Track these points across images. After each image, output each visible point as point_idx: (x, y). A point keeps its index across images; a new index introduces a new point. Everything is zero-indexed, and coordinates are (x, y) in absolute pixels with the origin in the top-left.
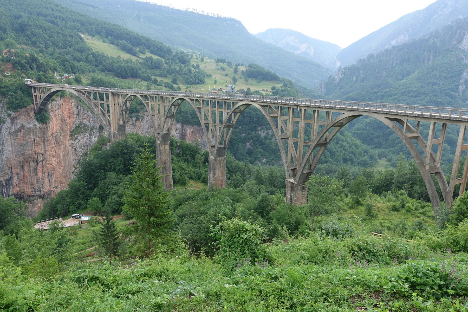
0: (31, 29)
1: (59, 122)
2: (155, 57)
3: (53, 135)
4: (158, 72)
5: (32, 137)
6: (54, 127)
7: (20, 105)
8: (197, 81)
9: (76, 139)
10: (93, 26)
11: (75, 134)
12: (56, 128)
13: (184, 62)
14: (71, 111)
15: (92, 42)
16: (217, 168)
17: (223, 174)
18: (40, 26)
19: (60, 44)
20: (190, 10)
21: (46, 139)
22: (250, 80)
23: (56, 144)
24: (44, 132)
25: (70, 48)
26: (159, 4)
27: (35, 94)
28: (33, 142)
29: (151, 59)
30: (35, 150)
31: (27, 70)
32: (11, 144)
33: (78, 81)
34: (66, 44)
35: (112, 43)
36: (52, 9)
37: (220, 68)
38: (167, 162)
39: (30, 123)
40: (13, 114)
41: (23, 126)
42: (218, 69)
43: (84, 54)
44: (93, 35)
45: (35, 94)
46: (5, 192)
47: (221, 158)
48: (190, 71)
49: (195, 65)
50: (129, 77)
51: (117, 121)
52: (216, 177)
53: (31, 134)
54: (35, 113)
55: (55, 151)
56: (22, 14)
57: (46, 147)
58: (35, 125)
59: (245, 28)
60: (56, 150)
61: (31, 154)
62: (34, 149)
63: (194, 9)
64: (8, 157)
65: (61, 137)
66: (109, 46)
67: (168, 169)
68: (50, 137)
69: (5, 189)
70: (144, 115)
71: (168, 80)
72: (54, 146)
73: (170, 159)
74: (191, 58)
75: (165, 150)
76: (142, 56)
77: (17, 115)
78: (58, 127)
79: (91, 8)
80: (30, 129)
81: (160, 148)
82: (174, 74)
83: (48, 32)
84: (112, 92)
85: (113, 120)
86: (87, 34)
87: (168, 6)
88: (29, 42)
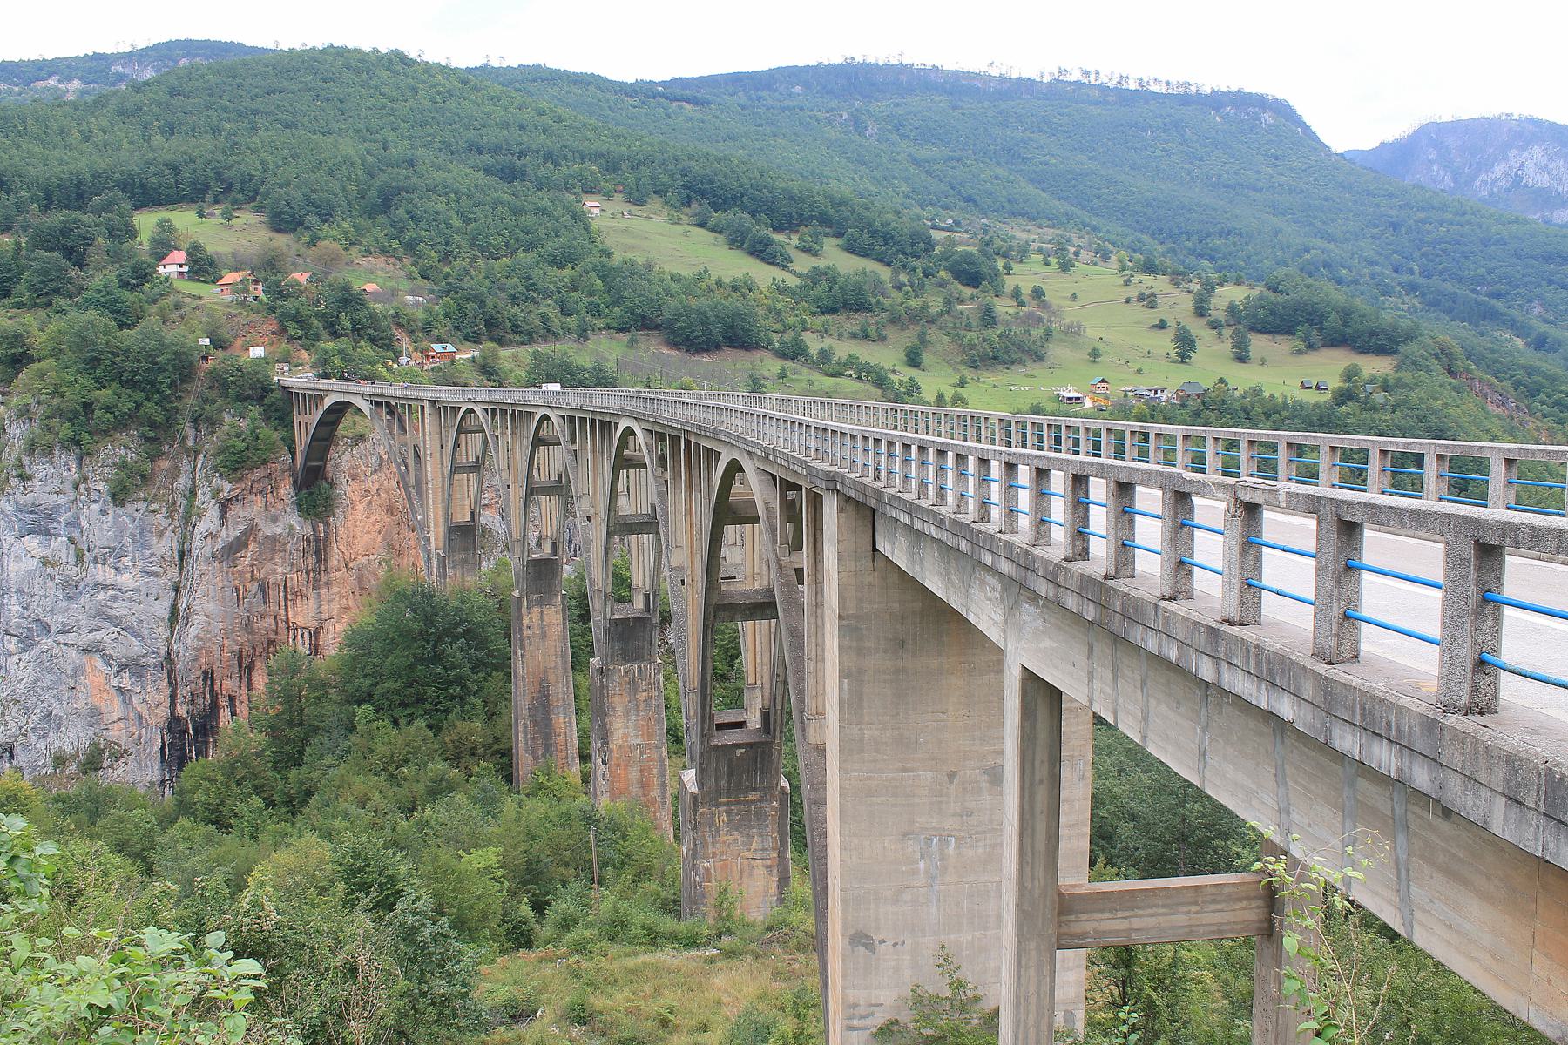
0: (410, 201)
1: (379, 515)
2: (846, 265)
3: (351, 564)
4: (854, 322)
5: (280, 570)
7: (248, 458)
10: (645, 171)
12: (367, 538)
15: (624, 224)
18: (445, 187)
19: (497, 241)
20: (1069, 78)
21: (324, 578)
22: (1259, 344)
23: (357, 597)
24: (320, 549)
25: (526, 251)
26: (949, 64)
28: (282, 588)
29: (830, 276)
30: (287, 615)
31: (317, 338)
33: (489, 372)
34: (517, 240)
35: (702, 225)
36: (522, 128)
38: (552, 678)
39: (275, 520)
40: (227, 486)
41: (251, 530)
42: (1128, 301)
43: (567, 271)
44: (640, 202)
49: (1026, 291)
50: (718, 347)
53: (278, 560)
54: (295, 482)
56: (421, 152)
57: (325, 608)
58: (291, 527)
62: (283, 612)
64: (202, 635)
66: (686, 235)
71: (887, 357)
72: (351, 603)
76: (803, 263)
77: (239, 490)
78: (374, 535)
79: (688, 107)
80: (274, 539)
81: (520, 618)
83: (465, 203)
84: (433, 402)
85: (435, 508)
86: (619, 197)
88: (395, 244)
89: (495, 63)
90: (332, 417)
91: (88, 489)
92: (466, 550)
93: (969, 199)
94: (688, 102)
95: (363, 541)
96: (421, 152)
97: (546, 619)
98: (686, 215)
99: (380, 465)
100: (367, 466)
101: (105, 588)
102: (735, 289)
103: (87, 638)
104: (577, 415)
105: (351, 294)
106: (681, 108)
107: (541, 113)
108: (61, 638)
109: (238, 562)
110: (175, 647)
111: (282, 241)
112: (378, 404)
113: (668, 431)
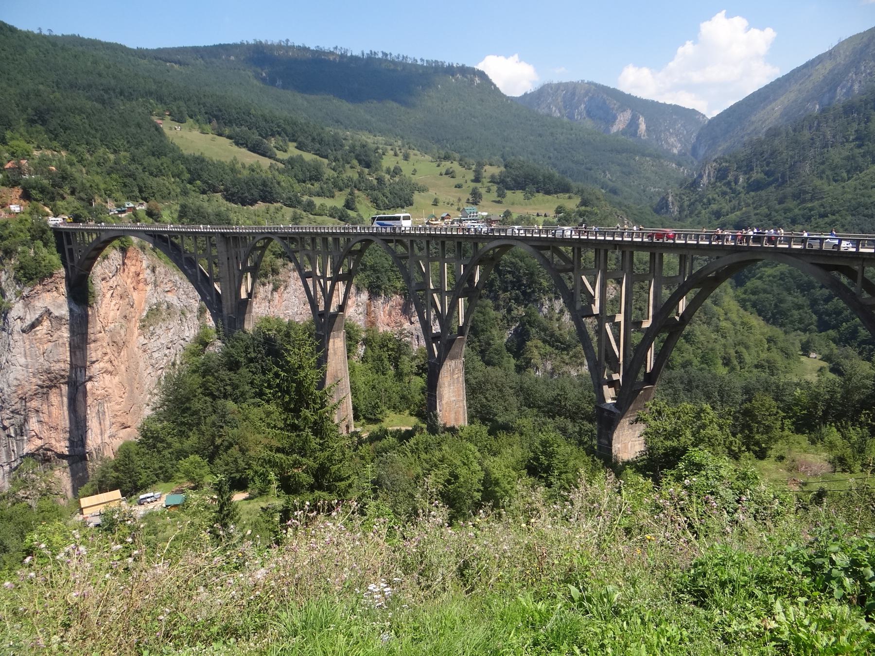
2: (308, 157)
3: (106, 328)
6: (108, 312)
8: (398, 201)
9: (152, 334)
11: (151, 325)
12: (112, 314)
13: (368, 165)
14: (141, 276)
17: (459, 395)
27: (70, 247)
32: (25, 351)
35: (220, 135)
36: (100, 75)
37: (444, 172)
42: (441, 175)
44: (181, 121)
45: (70, 247)
46: (13, 451)
48: (380, 180)
51: (233, 294)
55: (111, 362)
59: (495, 86)
60: (113, 358)
61: (63, 370)
63: (386, 55)
64: (19, 377)
65: (122, 332)
67: (342, 390)
68: (100, 332)
69: (15, 444)
70: (290, 277)
71: (338, 202)
72: (108, 351)
73: (345, 367)
74: (384, 154)
79: (176, 66)
82: (349, 190)
87: (332, 50)
90: (101, 245)
93: (337, 121)
94: (176, 63)
96: (41, 87)
97: (336, 344)
98: (208, 127)
99: (117, 272)
105: (67, 175)
106: (172, 66)
109: (38, 333)
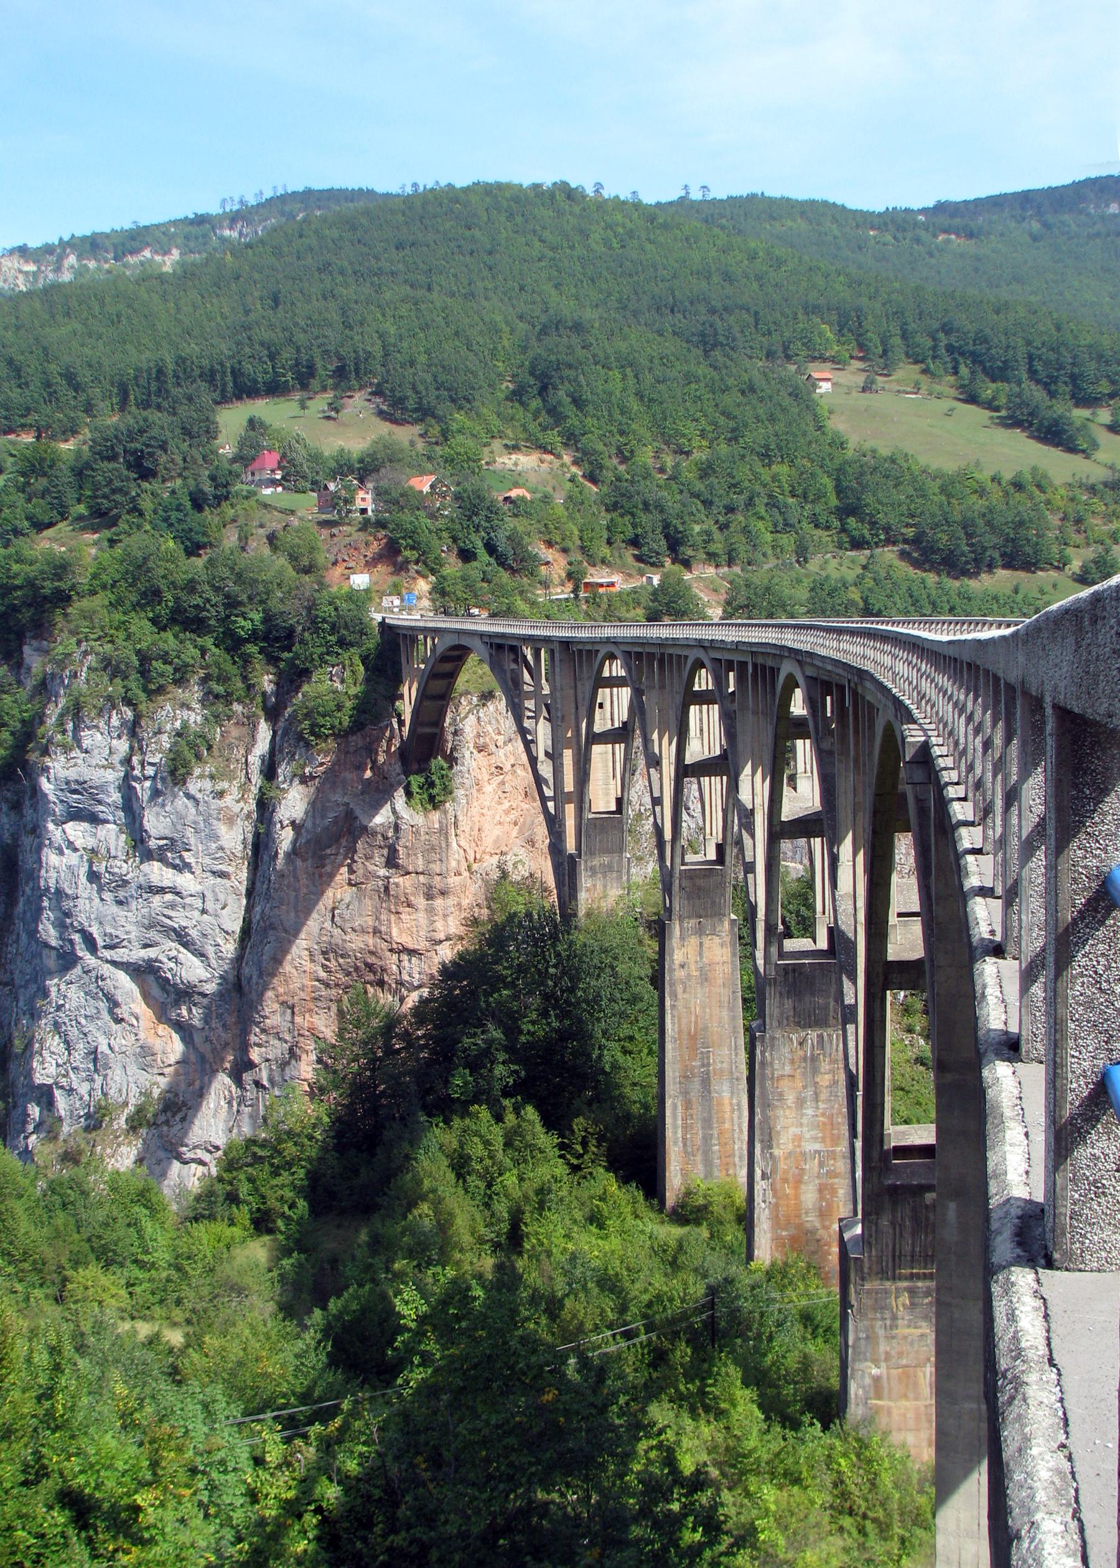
3: (475, 867)
6: (486, 827)
12: (497, 831)
16: (790, 1098)
35: (972, 399)
36: (728, 277)
47: (812, 1035)
52: (776, 1152)
57: (439, 925)
61: (372, 953)
68: (458, 873)
73: (733, 1019)
75: (701, 969)
78: (507, 827)
89: (696, 195)
90: (448, 667)
91: (142, 763)
92: (609, 851)
95: (490, 834)
100: (499, 733)
101: (162, 890)
102: (1018, 486)
103: (138, 954)
104: (736, 657)
107: (753, 257)
108: (107, 954)
110: (246, 971)
111: (405, 435)
112: (500, 647)
113: (835, 679)
